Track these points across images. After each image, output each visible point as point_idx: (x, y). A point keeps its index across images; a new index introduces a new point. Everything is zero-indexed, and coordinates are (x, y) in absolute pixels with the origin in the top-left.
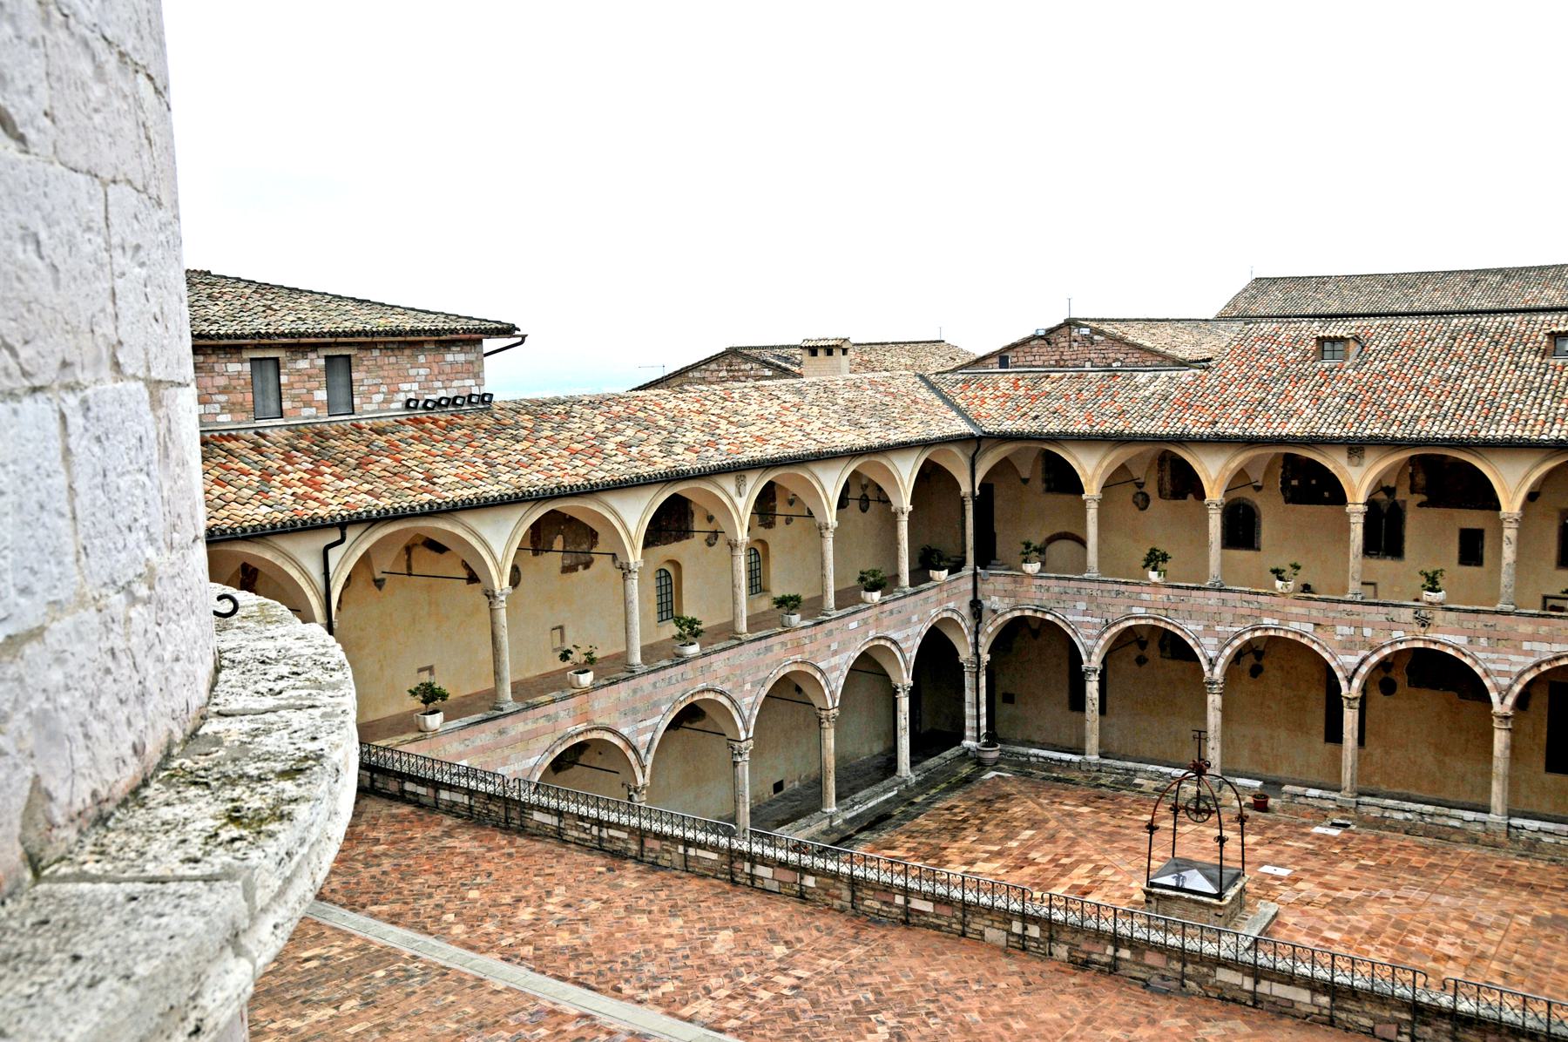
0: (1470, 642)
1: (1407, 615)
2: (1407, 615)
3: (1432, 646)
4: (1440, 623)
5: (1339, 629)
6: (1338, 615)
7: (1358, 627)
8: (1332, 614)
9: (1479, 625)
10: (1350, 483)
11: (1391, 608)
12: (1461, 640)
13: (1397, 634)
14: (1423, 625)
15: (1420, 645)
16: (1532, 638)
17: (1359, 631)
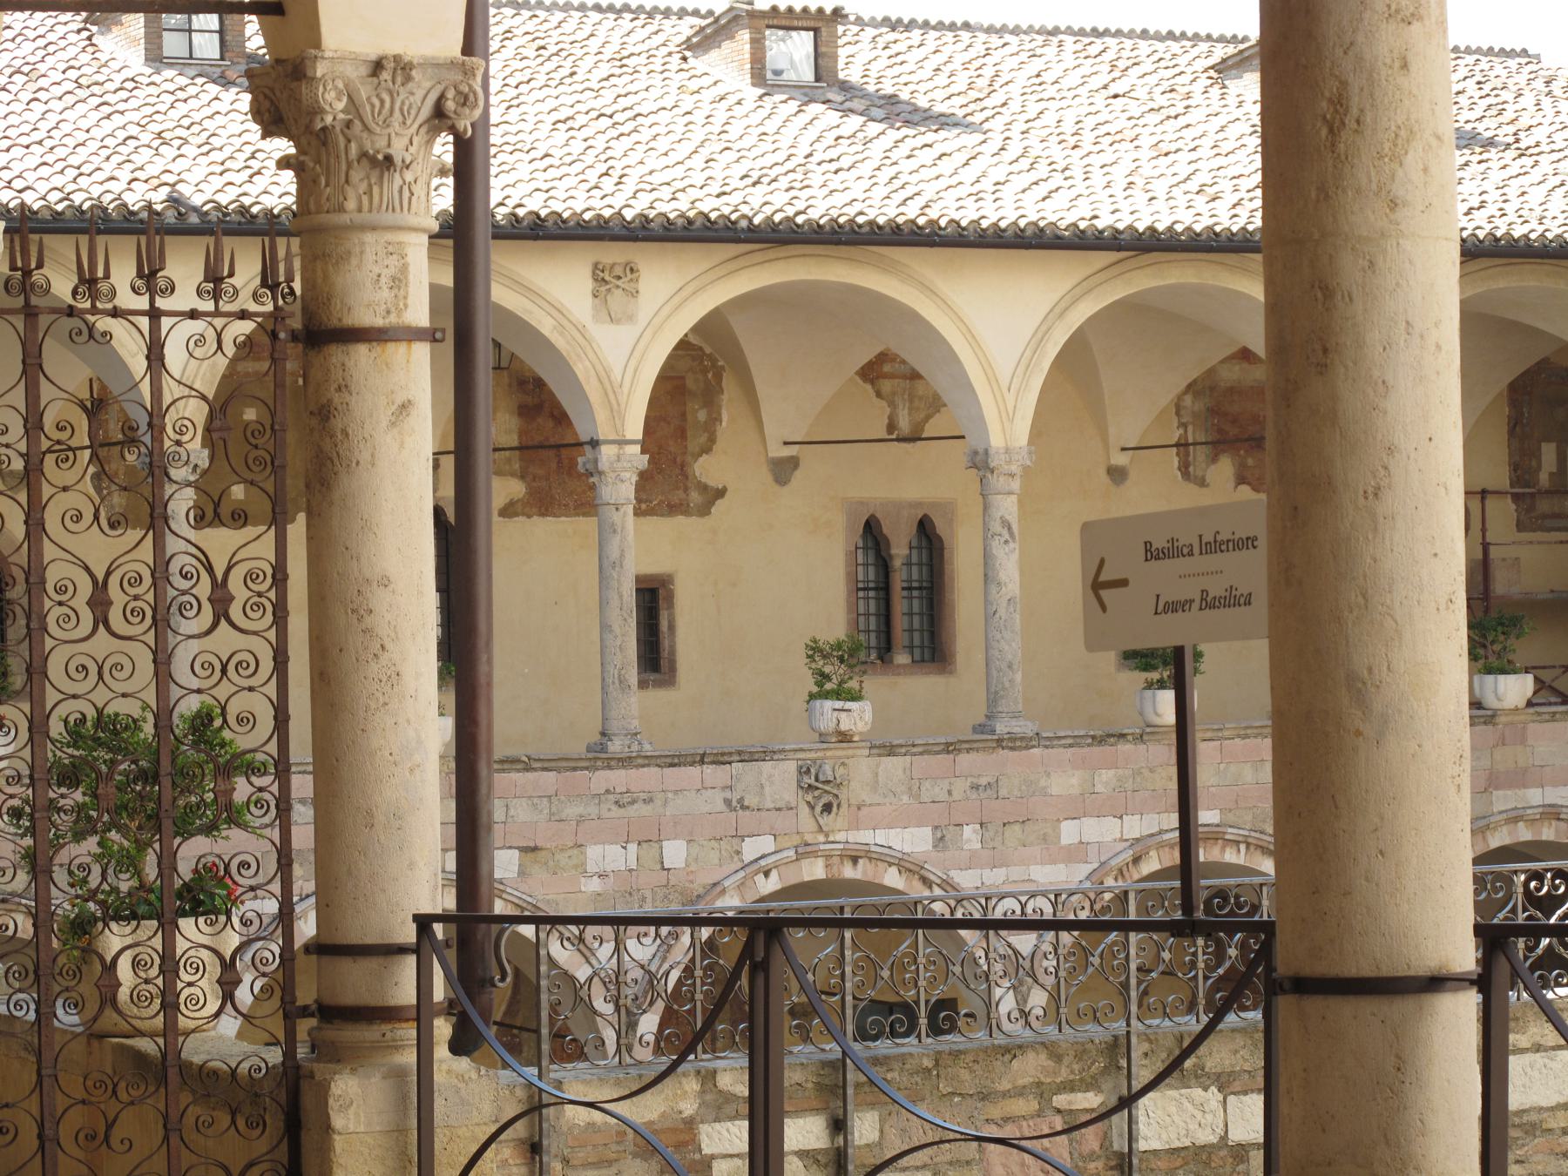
0: (940, 842)
1: (779, 780)
2: (779, 780)
3: (849, 872)
4: (866, 796)
5: (593, 852)
6: (593, 810)
7: (651, 839)
8: (572, 811)
9: (960, 787)
10: (604, 377)
11: (737, 767)
12: (914, 841)
13: (753, 848)
14: (827, 808)
15: (815, 870)
16: (1080, 808)
17: (650, 851)
